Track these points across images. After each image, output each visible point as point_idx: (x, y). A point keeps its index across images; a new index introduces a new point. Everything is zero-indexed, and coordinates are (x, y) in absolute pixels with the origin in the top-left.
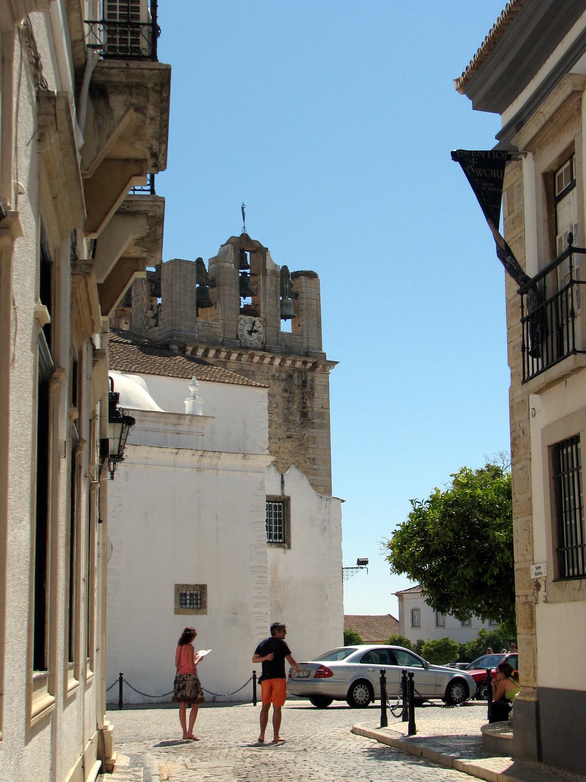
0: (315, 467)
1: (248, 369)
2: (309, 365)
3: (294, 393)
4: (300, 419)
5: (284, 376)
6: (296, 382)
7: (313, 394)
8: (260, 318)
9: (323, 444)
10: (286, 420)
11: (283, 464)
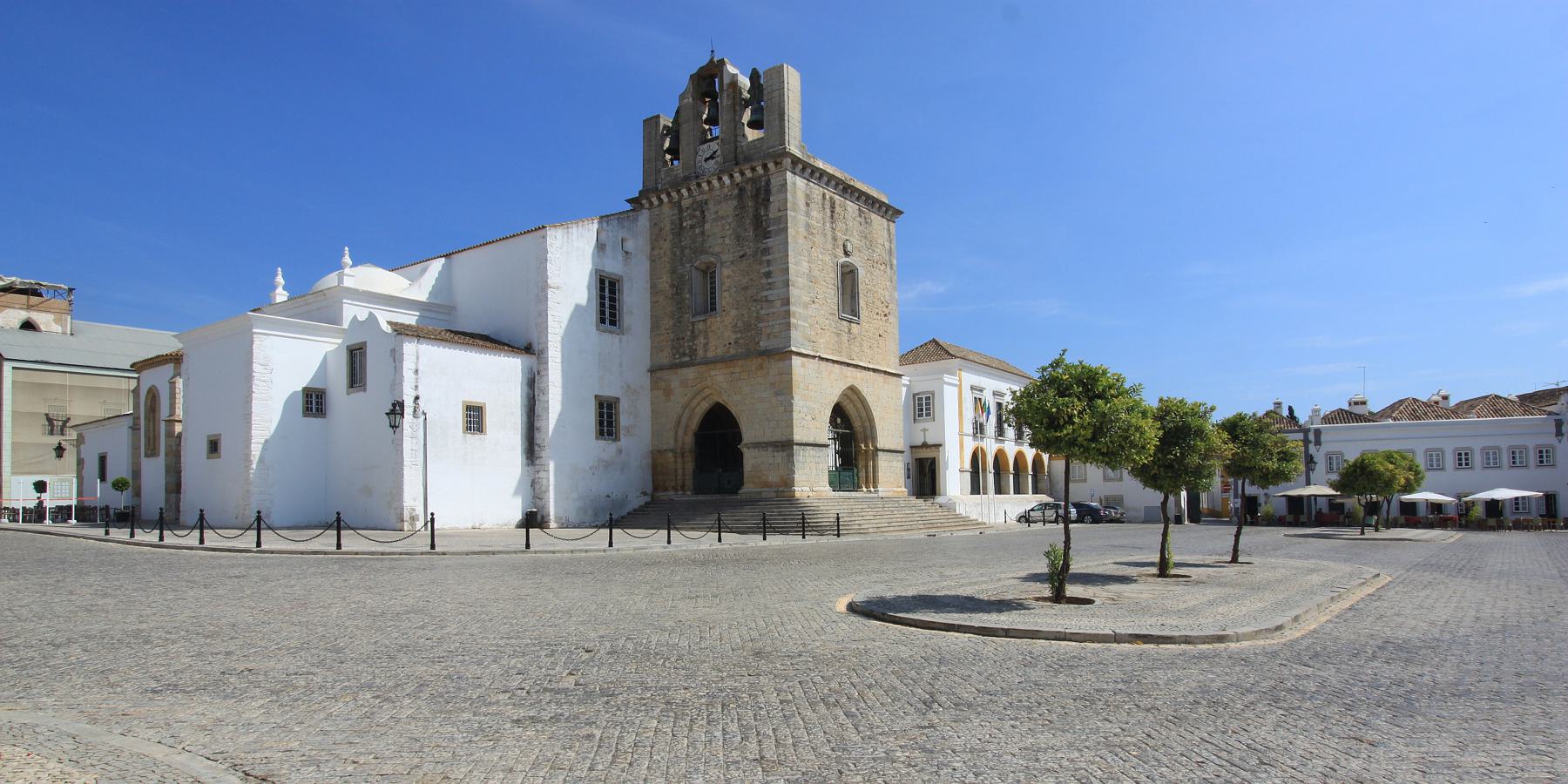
2: (760, 170)
5: (736, 191)
8: (717, 141)
10: (738, 238)
11: (735, 287)
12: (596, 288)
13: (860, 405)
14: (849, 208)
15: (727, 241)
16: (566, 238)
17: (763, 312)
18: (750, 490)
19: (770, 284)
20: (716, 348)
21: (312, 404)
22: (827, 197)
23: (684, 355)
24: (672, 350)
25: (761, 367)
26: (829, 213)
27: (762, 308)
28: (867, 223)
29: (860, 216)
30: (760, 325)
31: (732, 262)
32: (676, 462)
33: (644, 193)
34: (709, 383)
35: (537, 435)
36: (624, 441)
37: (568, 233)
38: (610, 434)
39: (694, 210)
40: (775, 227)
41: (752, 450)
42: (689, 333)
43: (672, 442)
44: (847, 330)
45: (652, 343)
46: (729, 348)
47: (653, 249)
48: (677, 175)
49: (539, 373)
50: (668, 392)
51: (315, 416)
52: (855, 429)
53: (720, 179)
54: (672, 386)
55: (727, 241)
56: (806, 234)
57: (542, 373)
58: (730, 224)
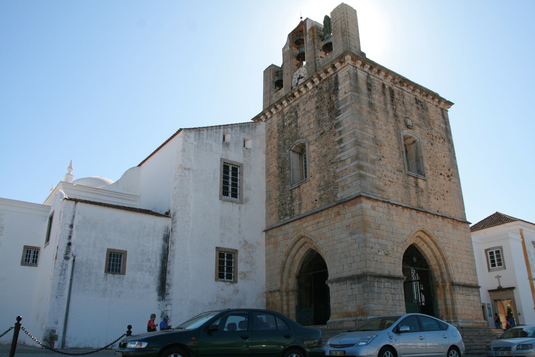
0: (342, 145)
1: (295, 104)
3: (324, 98)
4: (329, 115)
6: (324, 89)
7: (338, 89)
9: (347, 123)
10: (319, 122)
11: (318, 157)
12: (220, 171)
13: (433, 246)
14: (406, 97)
15: (312, 126)
16: (197, 136)
17: (338, 170)
18: (335, 320)
19: (342, 148)
20: (307, 207)
21: (29, 257)
22: (387, 87)
23: (286, 215)
24: (278, 213)
25: (338, 214)
26: (389, 98)
27: (337, 168)
28: (423, 108)
29: (417, 103)
30: (337, 181)
31: (316, 140)
32: (282, 300)
33: (263, 113)
34: (302, 233)
35: (168, 277)
36: (241, 283)
37: (199, 134)
38: (229, 277)
39: (291, 113)
40: (343, 106)
41: (334, 284)
42: (289, 198)
43: (279, 284)
44: (414, 185)
45: (267, 210)
46: (316, 203)
47: (267, 146)
48: (282, 95)
49: (172, 230)
50: (276, 244)
51: (30, 265)
52: (430, 268)
53: (306, 86)
54: (278, 241)
55: (312, 126)
56: (368, 109)
57: (174, 230)
58: (313, 115)
